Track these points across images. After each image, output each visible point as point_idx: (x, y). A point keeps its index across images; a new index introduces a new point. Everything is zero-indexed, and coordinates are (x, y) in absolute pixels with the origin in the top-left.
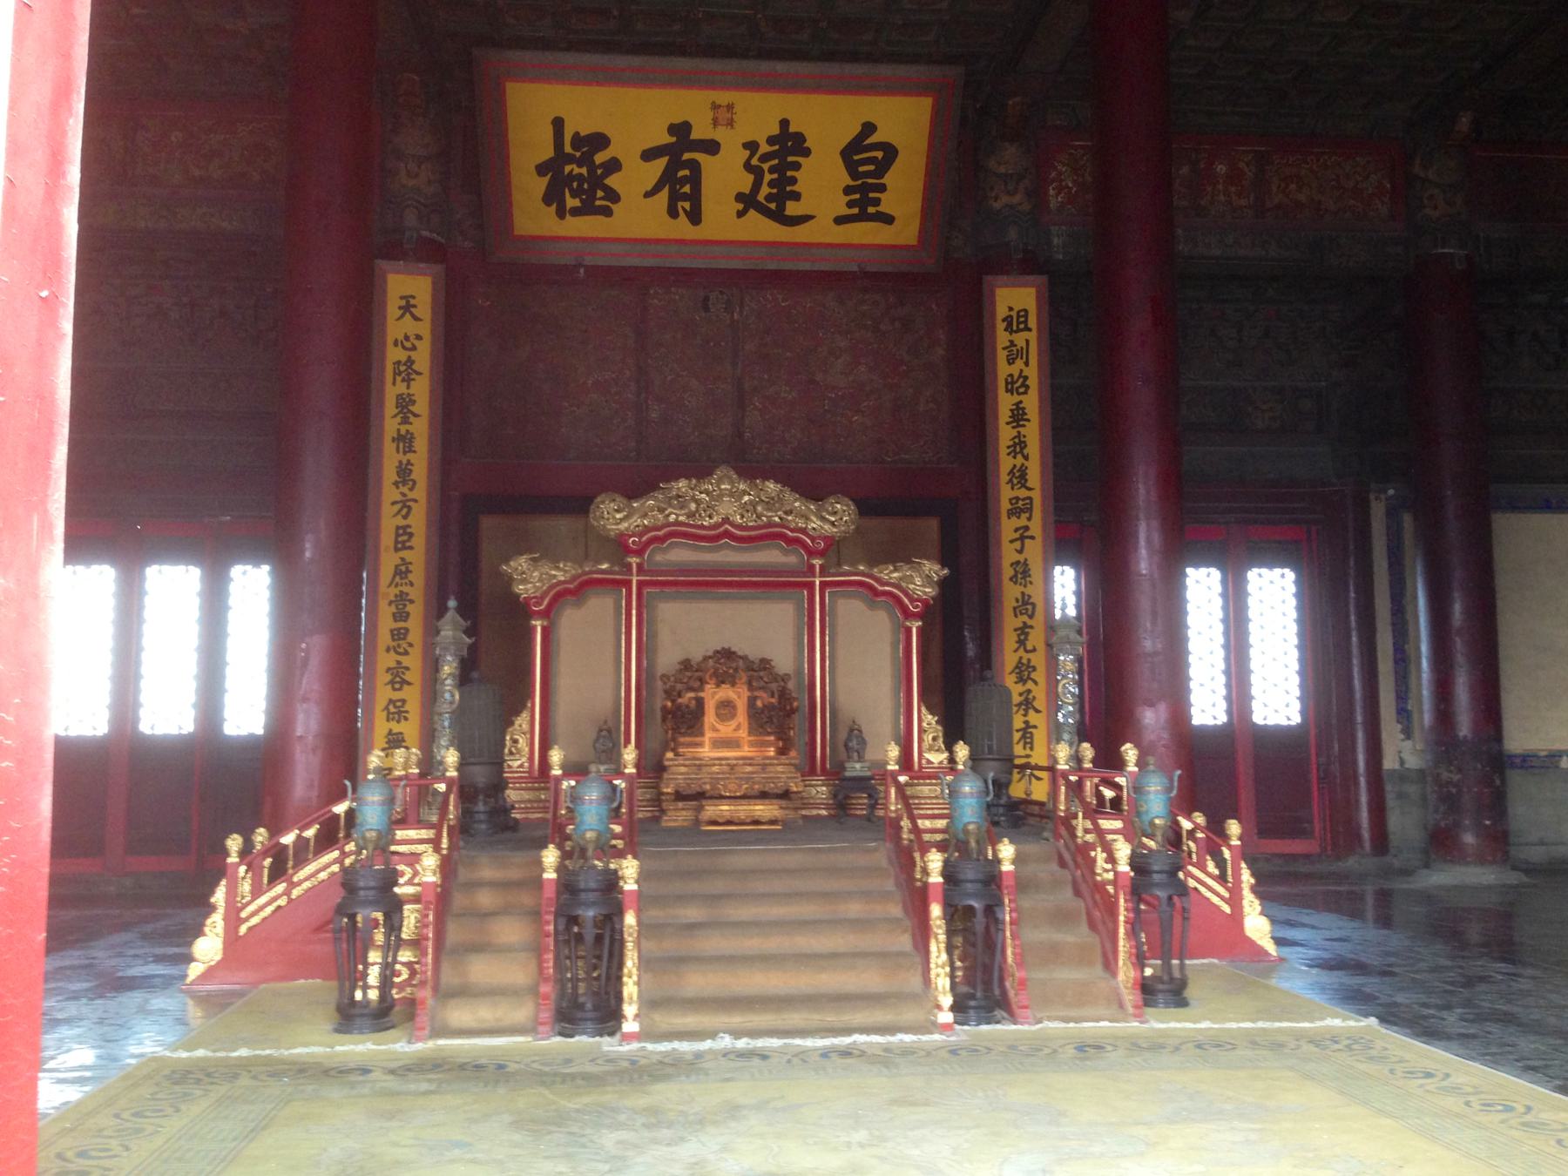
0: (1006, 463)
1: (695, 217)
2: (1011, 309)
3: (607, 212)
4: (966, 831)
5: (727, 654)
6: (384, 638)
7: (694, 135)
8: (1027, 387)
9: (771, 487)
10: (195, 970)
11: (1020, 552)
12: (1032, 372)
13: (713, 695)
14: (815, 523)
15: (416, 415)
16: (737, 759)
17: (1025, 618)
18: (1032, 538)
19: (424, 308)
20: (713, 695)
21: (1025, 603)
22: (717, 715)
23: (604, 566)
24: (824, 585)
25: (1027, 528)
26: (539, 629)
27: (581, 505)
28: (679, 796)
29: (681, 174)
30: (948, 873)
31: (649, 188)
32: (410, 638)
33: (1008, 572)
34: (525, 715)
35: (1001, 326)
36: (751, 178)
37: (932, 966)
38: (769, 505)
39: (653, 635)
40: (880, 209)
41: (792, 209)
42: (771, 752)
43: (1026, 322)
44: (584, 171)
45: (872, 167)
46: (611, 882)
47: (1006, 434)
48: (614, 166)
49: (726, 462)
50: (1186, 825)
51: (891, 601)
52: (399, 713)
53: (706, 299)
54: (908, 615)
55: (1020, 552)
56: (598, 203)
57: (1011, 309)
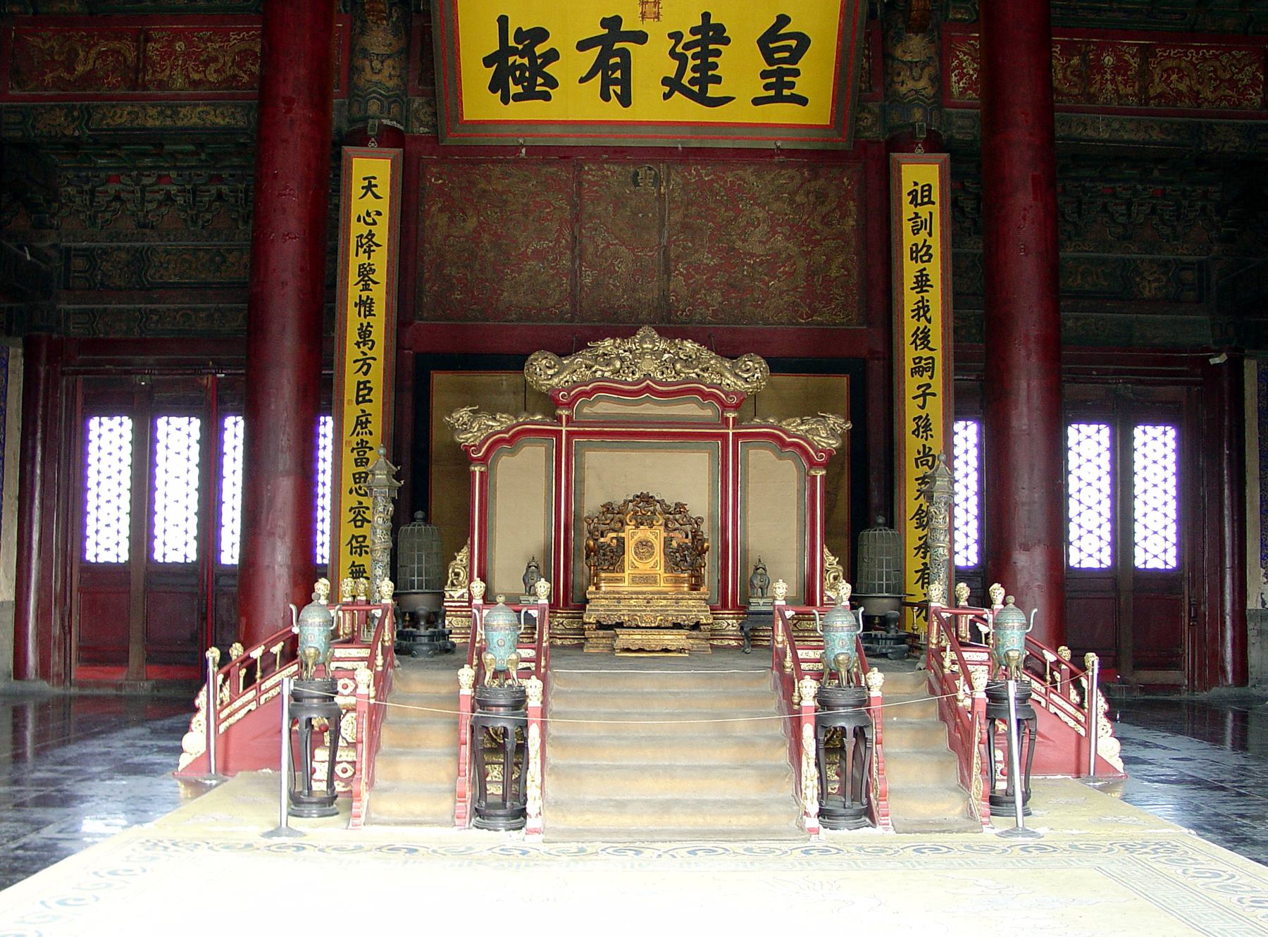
0: (910, 325)
1: (625, 100)
2: (916, 184)
3: (547, 97)
4: (836, 660)
5: (646, 499)
6: (348, 482)
8: (931, 256)
9: (688, 345)
10: (185, 760)
12: (935, 243)
13: (632, 535)
14: (729, 380)
16: (652, 593)
18: (934, 395)
19: (384, 189)
20: (632, 535)
23: (538, 417)
25: (929, 386)
27: (516, 362)
28: (600, 626)
29: (611, 61)
30: (823, 701)
33: (910, 426)
34: (465, 550)
35: (906, 199)
37: (803, 779)
38: (688, 362)
39: (581, 481)
41: (713, 91)
42: (686, 587)
44: (526, 61)
45: (787, 54)
46: (519, 702)
47: (910, 299)
48: (552, 55)
49: (650, 323)
50: (1050, 657)
51: (798, 451)
52: (361, 547)
54: (813, 464)
55: (922, 407)
56: (538, 89)
57: (916, 184)
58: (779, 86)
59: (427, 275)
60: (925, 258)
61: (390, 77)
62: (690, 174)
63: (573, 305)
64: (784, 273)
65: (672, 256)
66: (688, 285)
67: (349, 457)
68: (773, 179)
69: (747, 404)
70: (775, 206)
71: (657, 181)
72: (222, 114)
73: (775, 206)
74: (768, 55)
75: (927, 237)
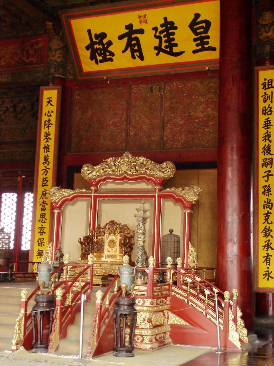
1: (142, 58)
2: (265, 79)
3: (111, 60)
5: (112, 223)
6: (38, 217)
7: (134, 28)
8: (272, 112)
9: (141, 159)
11: (267, 181)
13: (108, 238)
15: (50, 139)
17: (268, 209)
19: (54, 102)
20: (108, 238)
21: (268, 203)
22: (109, 245)
23: (84, 190)
24: (160, 197)
25: (270, 171)
26: (56, 213)
31: (123, 49)
32: (46, 217)
35: (261, 87)
36: (158, 40)
40: (209, 45)
41: (175, 50)
43: (271, 84)
44: (101, 46)
45: (202, 30)
48: (110, 43)
52: (42, 243)
53: (152, 87)
55: (267, 181)
56: (108, 57)
57: (265, 79)
58: (202, 44)
59: (73, 135)
60: (269, 113)
61: (59, 57)
62: (173, 85)
63: (126, 144)
64: (211, 124)
65: (165, 121)
66: (171, 133)
67: (39, 207)
68: (208, 84)
69: (165, 183)
70: (208, 96)
71: (160, 90)
72: (4, 77)
73: (208, 96)
74: (194, 31)
75: (270, 103)
